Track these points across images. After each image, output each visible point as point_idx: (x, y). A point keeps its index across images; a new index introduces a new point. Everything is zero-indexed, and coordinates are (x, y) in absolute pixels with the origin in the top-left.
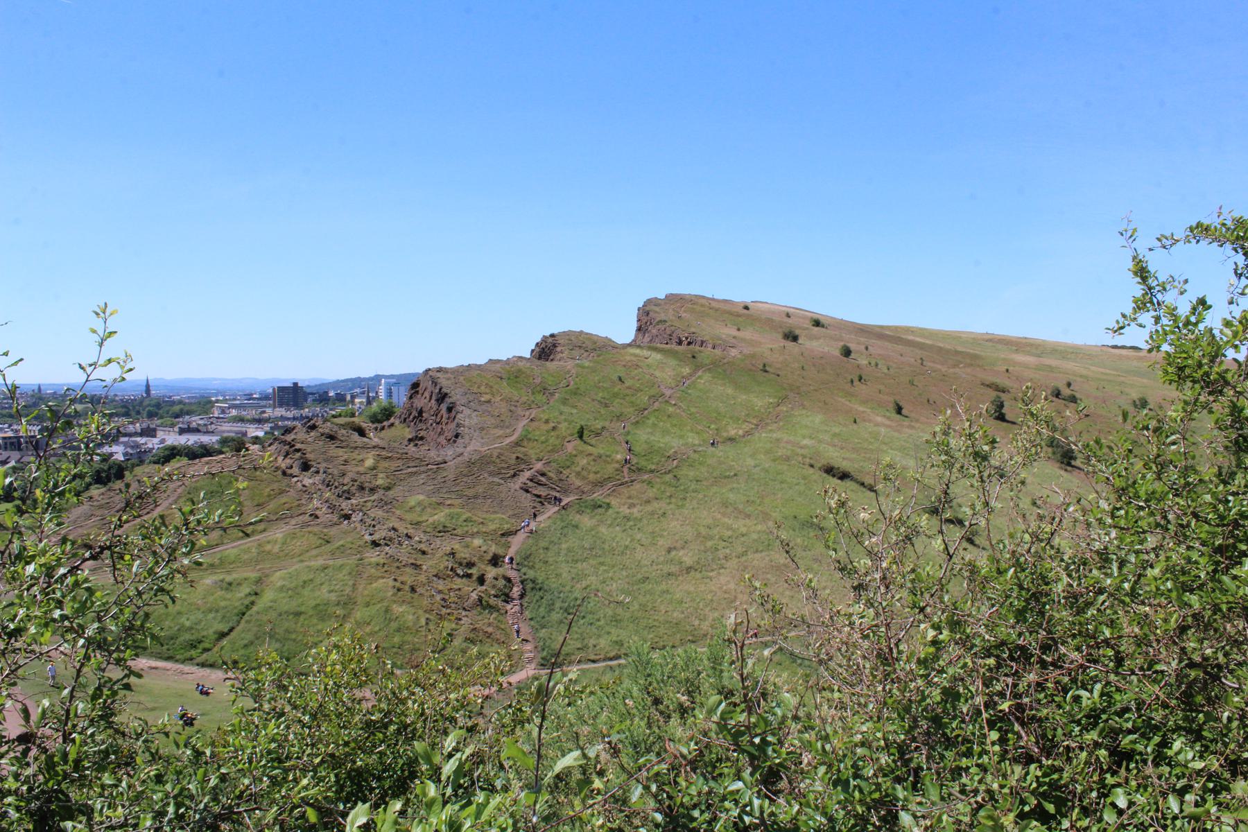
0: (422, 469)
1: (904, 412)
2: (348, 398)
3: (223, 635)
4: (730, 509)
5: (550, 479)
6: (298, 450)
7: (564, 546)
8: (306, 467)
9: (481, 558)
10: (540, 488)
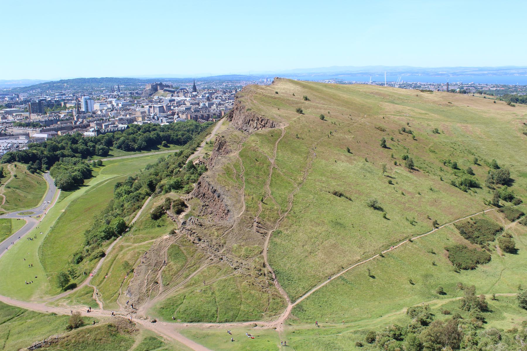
0: (229, 231)
1: (351, 151)
2: (63, 105)
3: (217, 311)
4: (313, 223)
5: (262, 224)
6: (194, 233)
7: (277, 254)
8: (200, 240)
9: (260, 266)
10: (262, 229)
